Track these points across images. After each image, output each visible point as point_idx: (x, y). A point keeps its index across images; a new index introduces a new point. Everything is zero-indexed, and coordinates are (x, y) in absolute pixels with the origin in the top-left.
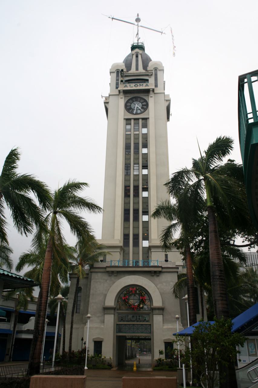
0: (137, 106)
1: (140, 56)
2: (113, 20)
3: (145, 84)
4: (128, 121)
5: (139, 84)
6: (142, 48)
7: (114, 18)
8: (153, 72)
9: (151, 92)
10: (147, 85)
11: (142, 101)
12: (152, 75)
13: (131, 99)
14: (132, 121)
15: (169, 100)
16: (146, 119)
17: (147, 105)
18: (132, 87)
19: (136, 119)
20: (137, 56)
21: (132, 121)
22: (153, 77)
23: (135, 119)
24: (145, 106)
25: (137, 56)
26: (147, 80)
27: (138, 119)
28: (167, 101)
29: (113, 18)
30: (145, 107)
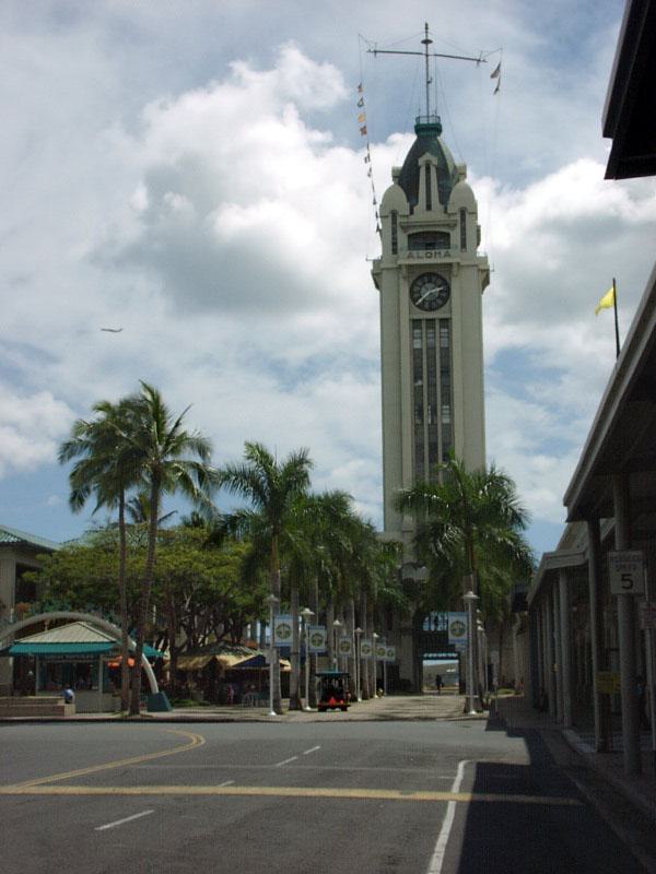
0: (429, 292)
1: (433, 171)
2: (378, 54)
3: (443, 252)
4: (416, 323)
5: (433, 252)
6: (437, 129)
7: (378, 49)
8: (458, 217)
9: (455, 269)
10: (448, 255)
11: (439, 282)
12: (456, 225)
13: (420, 277)
14: (424, 324)
15: (487, 271)
16: (446, 322)
17: (448, 291)
18: (422, 258)
19: (431, 322)
20: (428, 169)
21: (424, 324)
22: (458, 229)
23: (427, 320)
24: (445, 296)
25: (428, 169)
26: (448, 235)
27: (433, 320)
28: (483, 271)
29: (375, 52)
30: (444, 295)
